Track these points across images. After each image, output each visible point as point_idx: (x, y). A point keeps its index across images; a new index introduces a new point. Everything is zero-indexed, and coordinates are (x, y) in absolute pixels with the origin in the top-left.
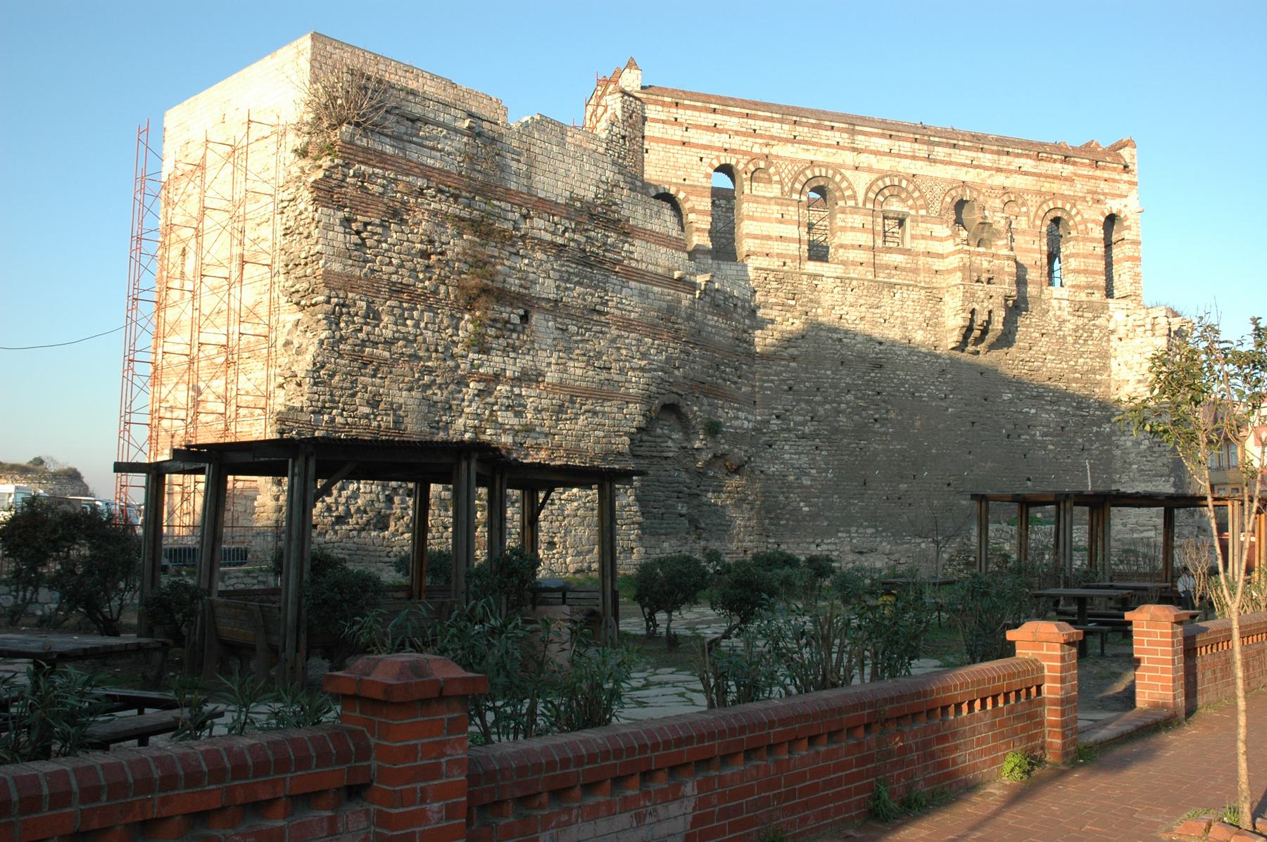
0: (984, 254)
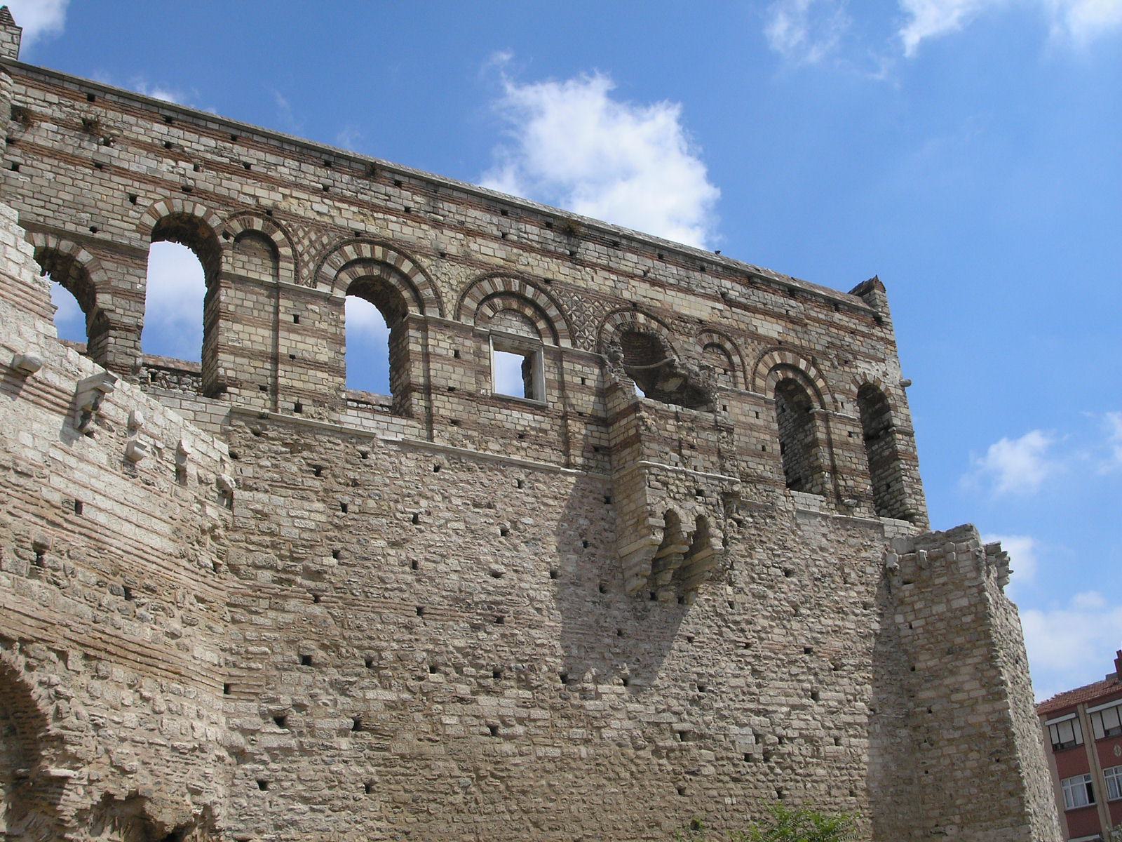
0: (677, 417)
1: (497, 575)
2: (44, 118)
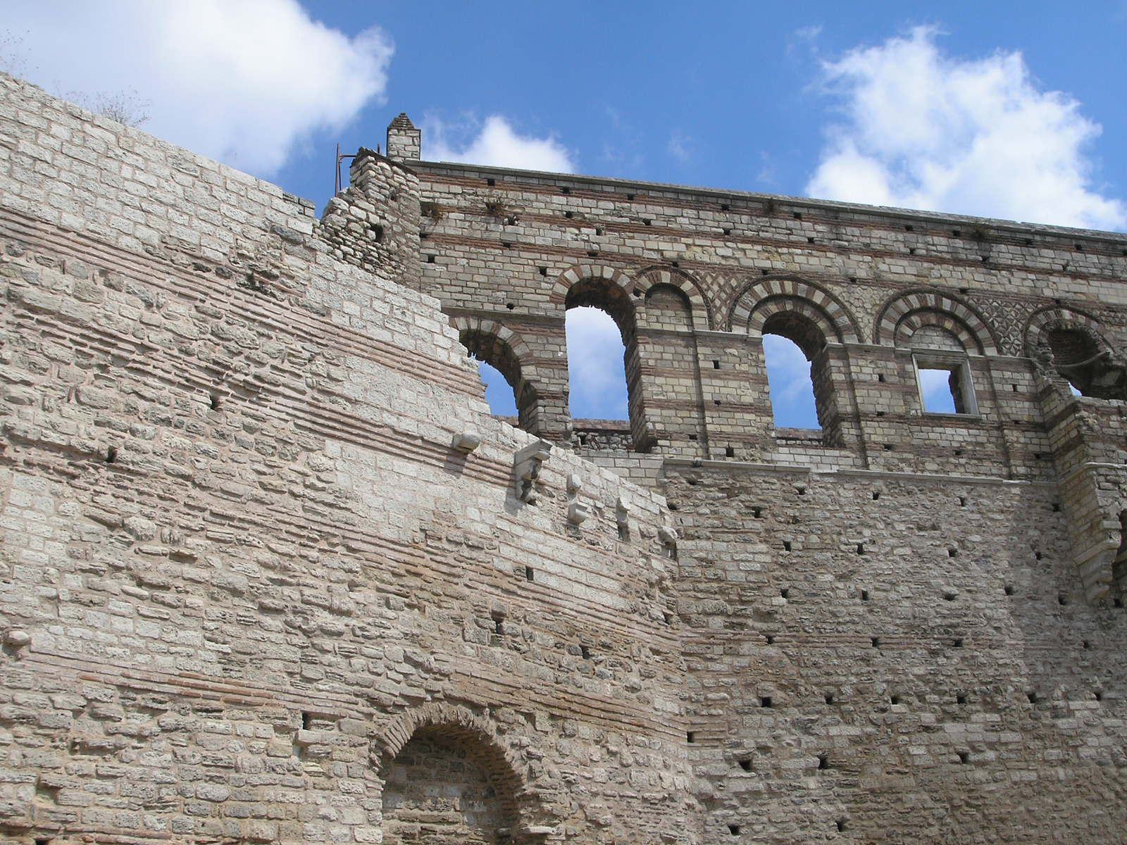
1: (950, 597)
2: (451, 209)
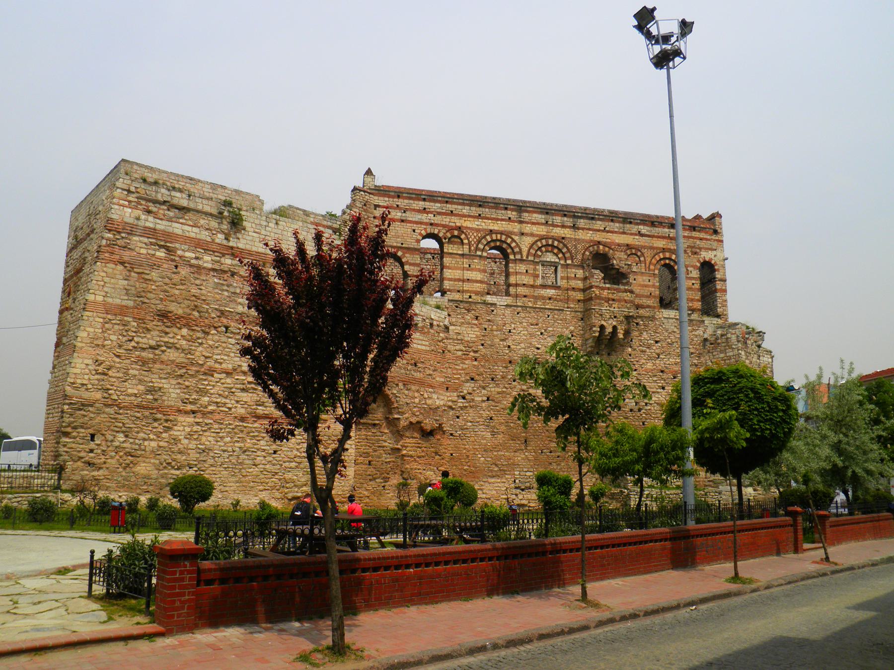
0: (608, 289)
1: (538, 349)
